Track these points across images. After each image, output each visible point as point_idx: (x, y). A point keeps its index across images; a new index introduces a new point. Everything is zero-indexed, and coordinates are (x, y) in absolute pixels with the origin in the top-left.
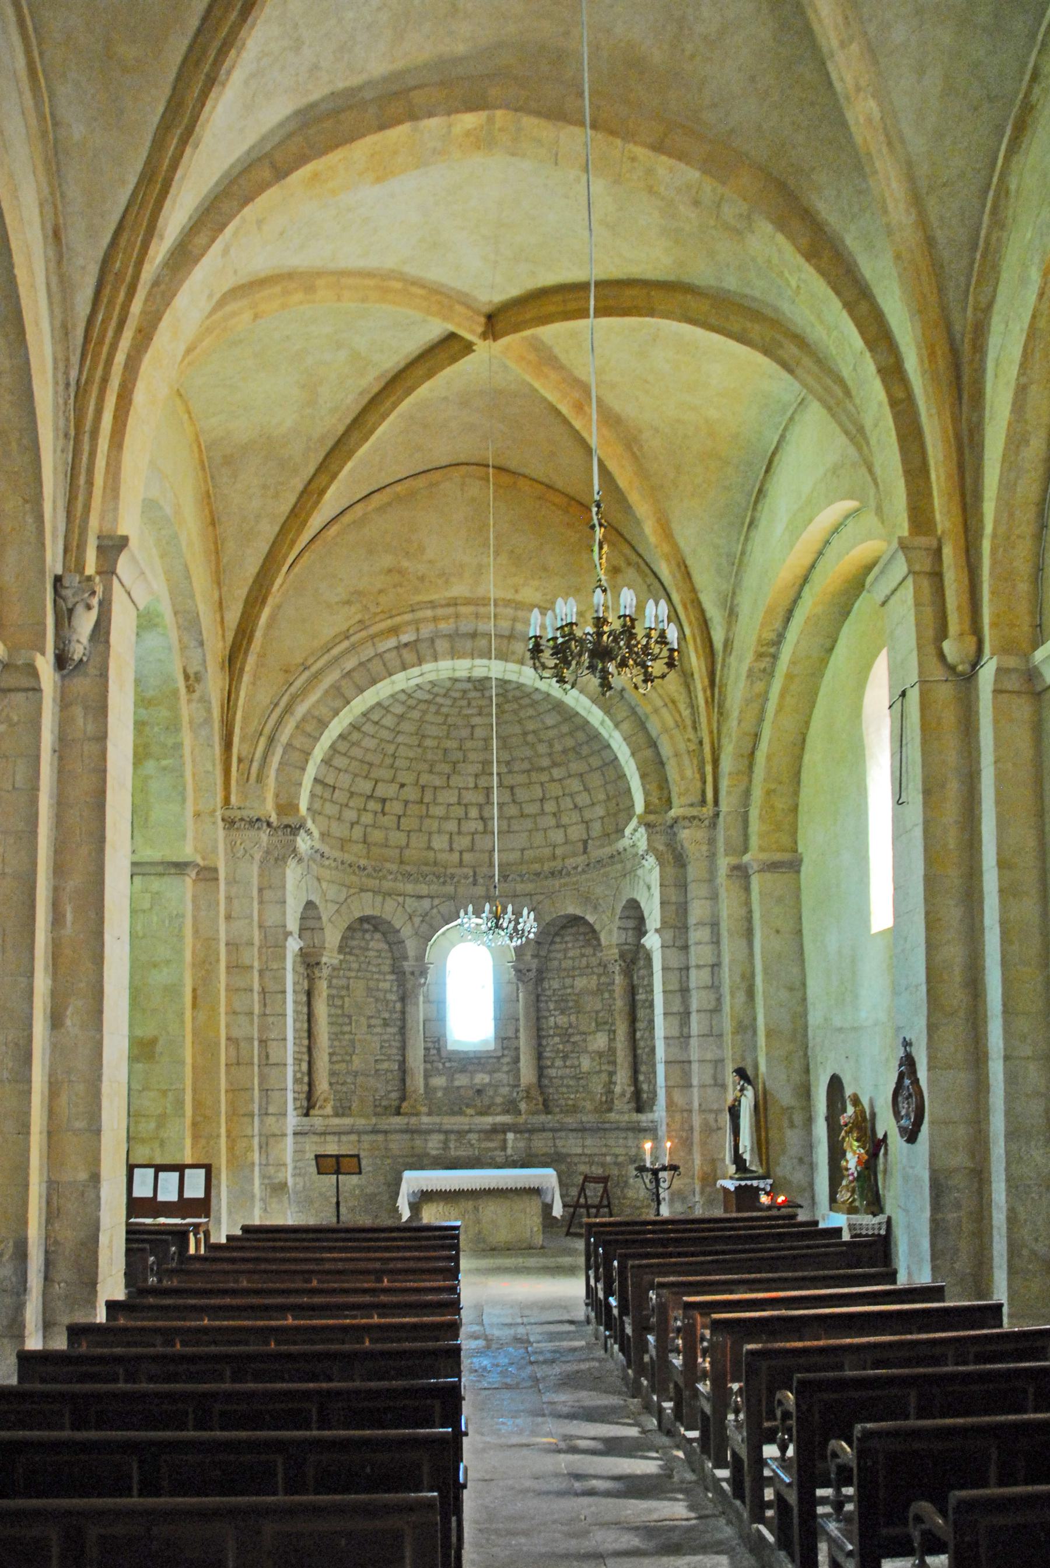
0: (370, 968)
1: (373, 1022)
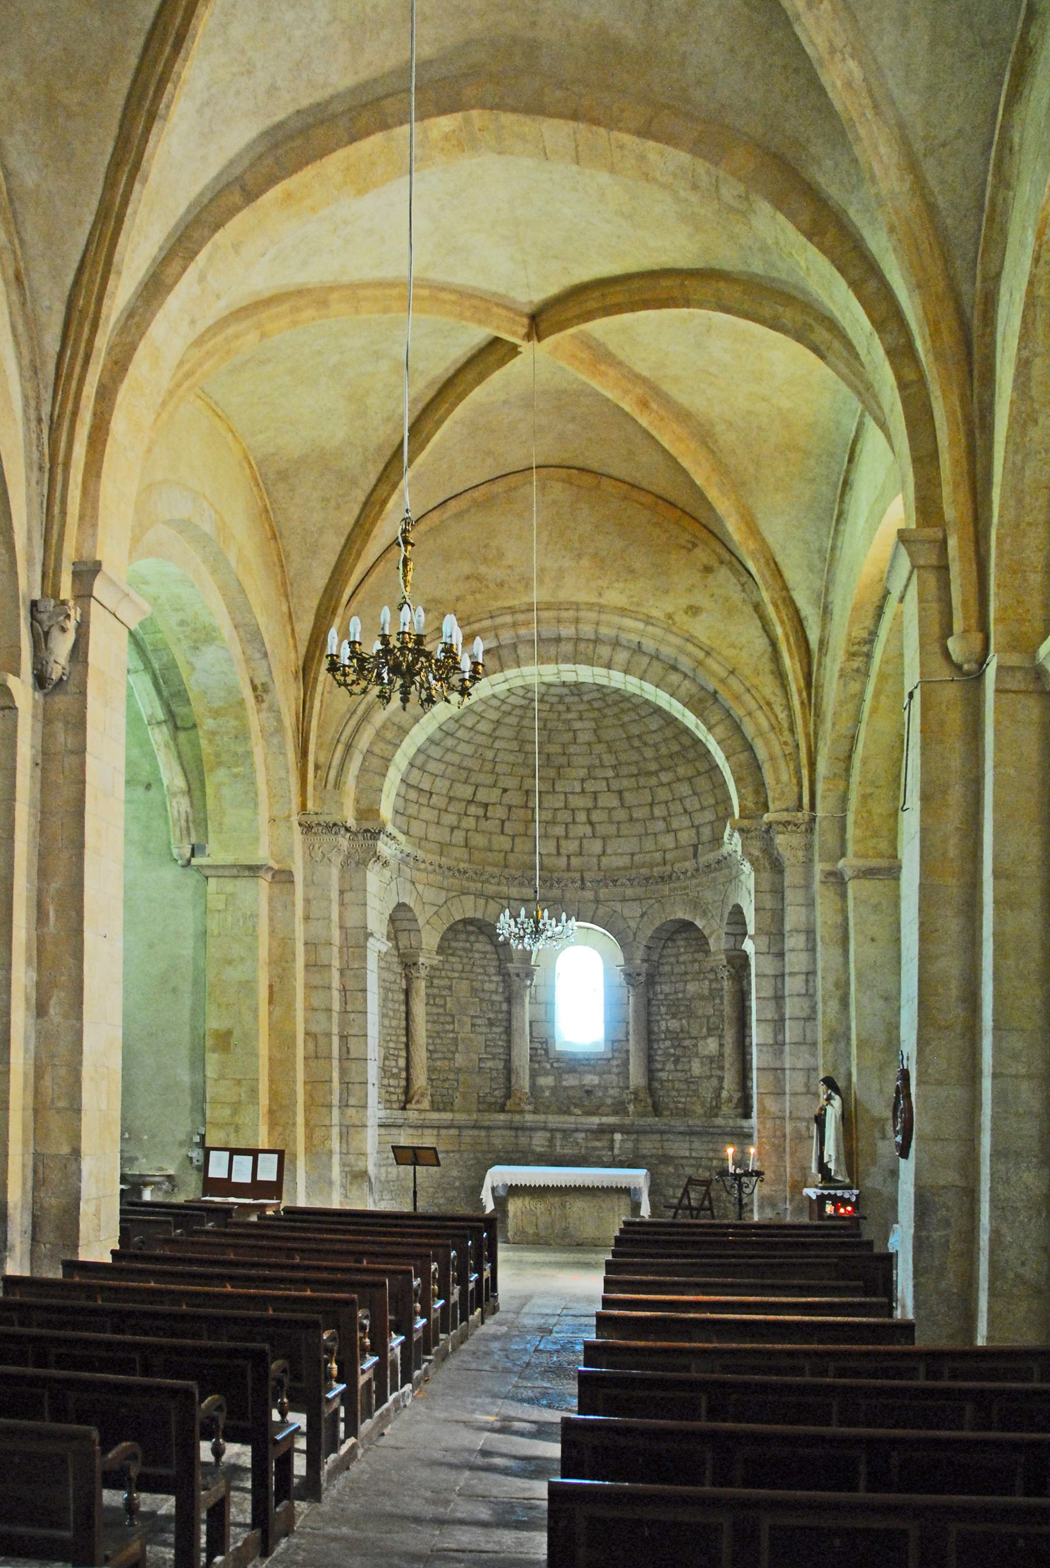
0: (475, 969)
1: (478, 1021)
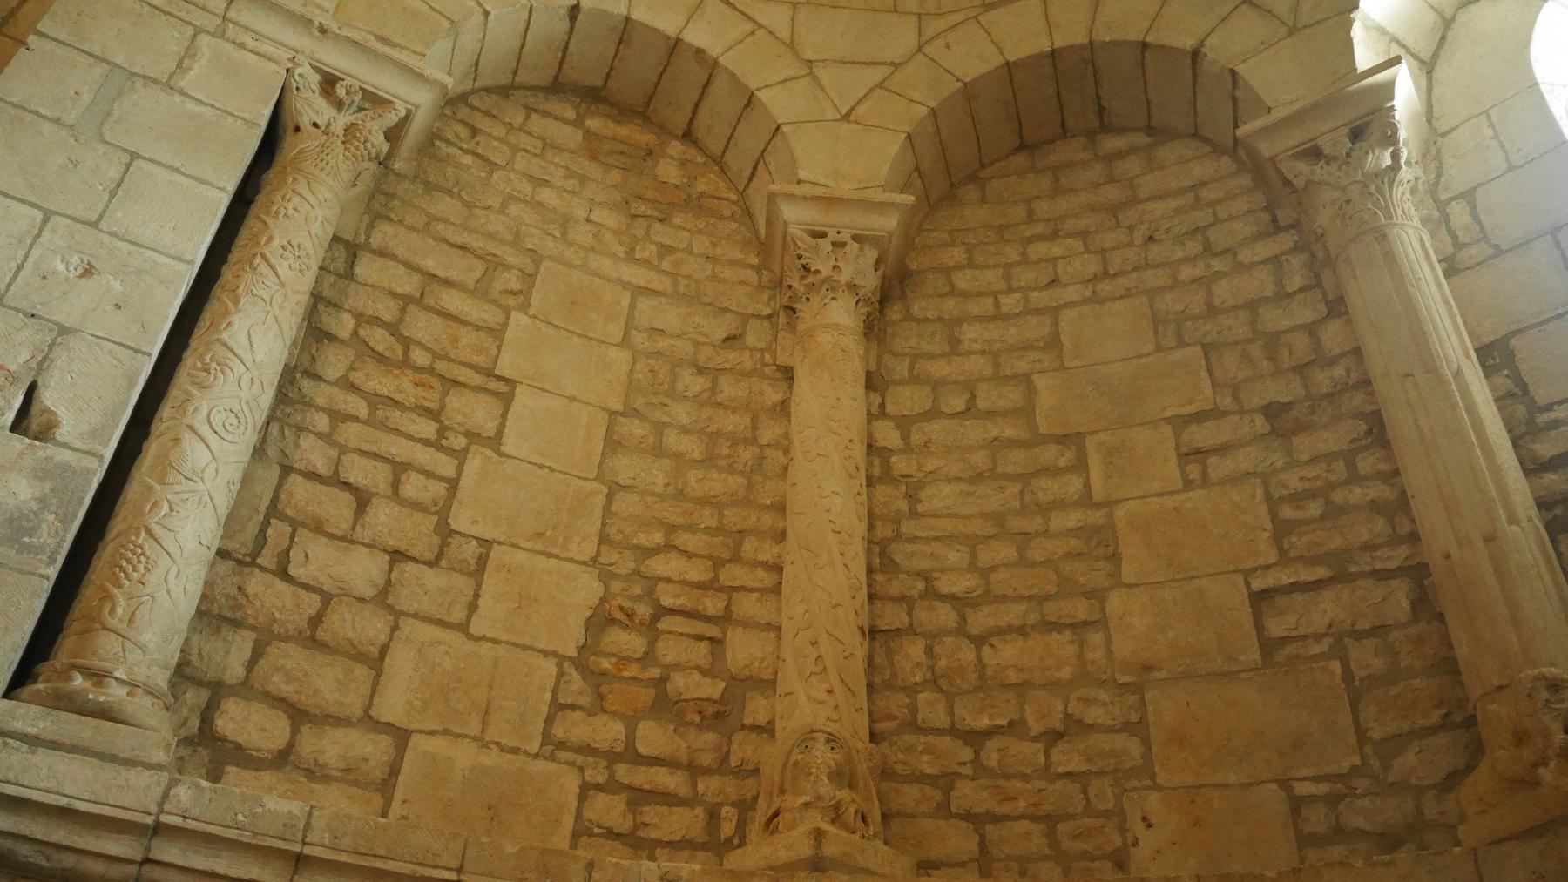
1: (1203, 435)
